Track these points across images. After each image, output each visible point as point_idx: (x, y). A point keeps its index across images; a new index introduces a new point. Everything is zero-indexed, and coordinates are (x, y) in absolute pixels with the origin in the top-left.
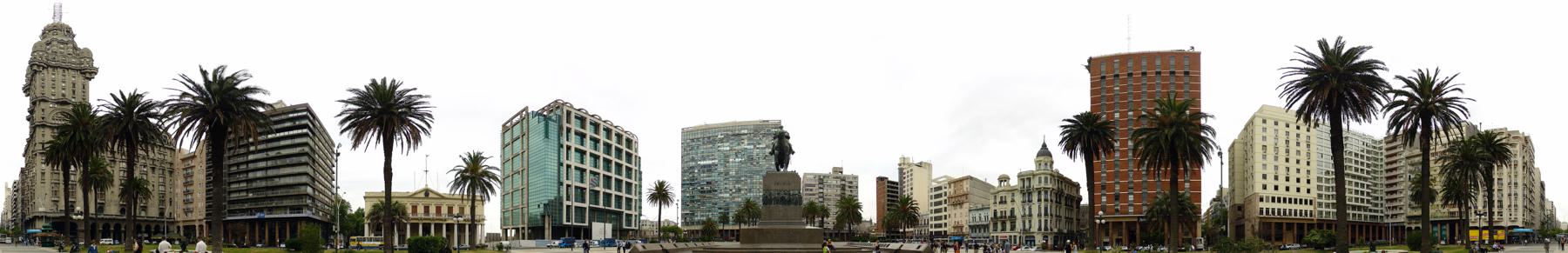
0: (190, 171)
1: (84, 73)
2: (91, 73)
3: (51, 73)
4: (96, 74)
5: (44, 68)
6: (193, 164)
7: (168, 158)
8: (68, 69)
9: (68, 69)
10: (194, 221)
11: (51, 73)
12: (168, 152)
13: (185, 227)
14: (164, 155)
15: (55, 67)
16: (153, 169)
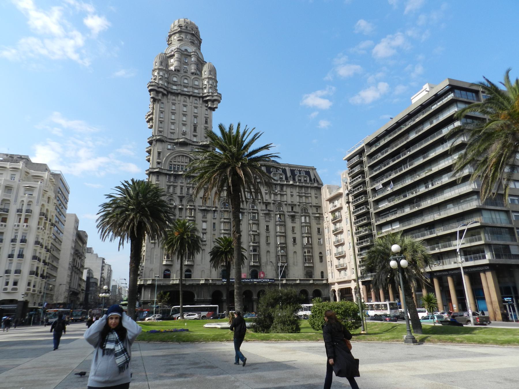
0: (337, 214)
1: (206, 102)
2: (213, 101)
3: (171, 101)
4: (219, 102)
5: (164, 95)
6: (338, 206)
7: (314, 202)
8: (189, 96)
9: (189, 96)
10: (349, 282)
11: (171, 101)
12: (313, 192)
13: (341, 290)
15: (177, 94)
16: (293, 217)
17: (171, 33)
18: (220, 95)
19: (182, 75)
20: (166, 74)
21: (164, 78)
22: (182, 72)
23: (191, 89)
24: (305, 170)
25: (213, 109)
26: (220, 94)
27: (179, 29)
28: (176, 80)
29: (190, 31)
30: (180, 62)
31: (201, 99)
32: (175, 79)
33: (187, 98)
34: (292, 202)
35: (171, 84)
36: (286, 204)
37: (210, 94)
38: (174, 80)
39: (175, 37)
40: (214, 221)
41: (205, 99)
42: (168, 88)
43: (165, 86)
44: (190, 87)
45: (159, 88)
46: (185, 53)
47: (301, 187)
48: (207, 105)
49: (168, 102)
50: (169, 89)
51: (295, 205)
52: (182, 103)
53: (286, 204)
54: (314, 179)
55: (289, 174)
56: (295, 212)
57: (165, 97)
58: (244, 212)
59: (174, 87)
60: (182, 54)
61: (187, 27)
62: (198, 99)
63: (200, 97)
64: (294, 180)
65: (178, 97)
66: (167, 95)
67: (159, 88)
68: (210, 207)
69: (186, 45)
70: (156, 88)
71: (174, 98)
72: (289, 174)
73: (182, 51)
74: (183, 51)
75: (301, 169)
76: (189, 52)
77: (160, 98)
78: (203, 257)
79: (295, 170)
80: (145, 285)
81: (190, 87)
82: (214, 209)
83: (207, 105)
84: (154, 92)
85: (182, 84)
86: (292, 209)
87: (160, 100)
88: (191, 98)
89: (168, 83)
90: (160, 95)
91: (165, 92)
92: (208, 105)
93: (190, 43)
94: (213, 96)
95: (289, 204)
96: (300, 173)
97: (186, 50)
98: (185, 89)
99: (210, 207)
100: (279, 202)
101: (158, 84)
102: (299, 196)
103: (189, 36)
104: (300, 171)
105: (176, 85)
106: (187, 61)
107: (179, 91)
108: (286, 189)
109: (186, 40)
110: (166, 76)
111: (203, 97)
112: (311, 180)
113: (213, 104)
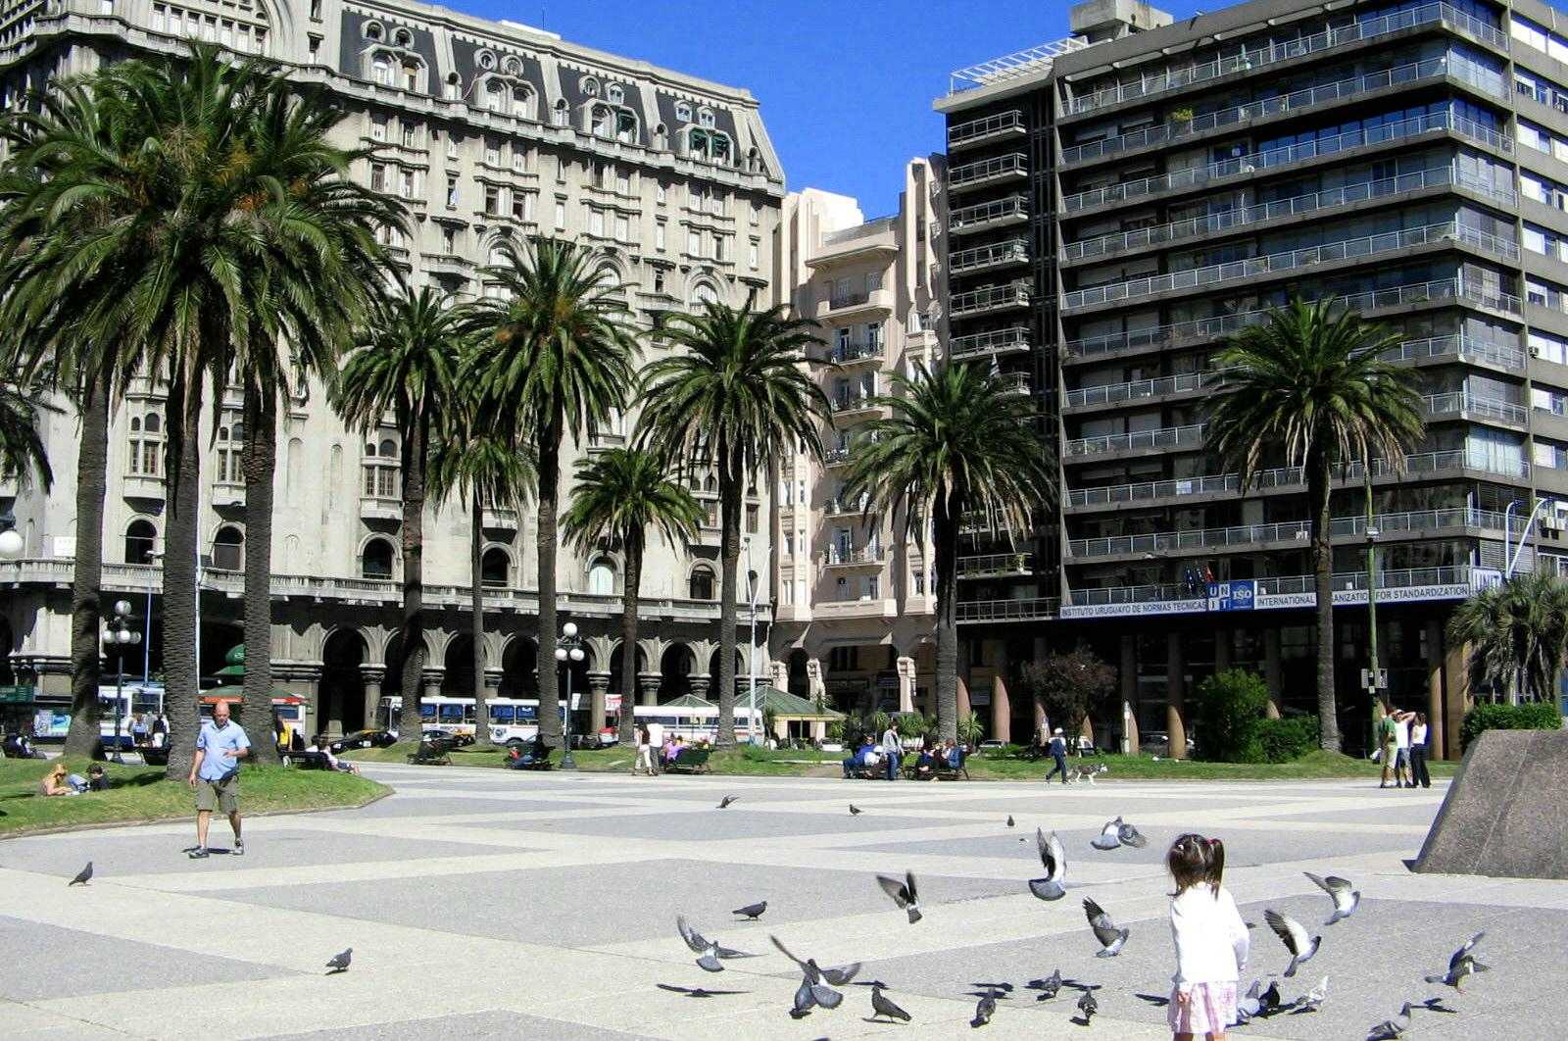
14: (719, 236)
24: (714, 103)
34: (660, 251)
36: (636, 260)
47: (700, 186)
51: (670, 267)
53: (636, 260)
54: (753, 153)
55: (653, 118)
56: (669, 299)
58: (468, 280)
64: (674, 146)
72: (653, 118)
75: (697, 99)
78: (293, 476)
79: (675, 98)
80: (58, 586)
86: (659, 284)
95: (648, 261)
96: (695, 120)
100: (611, 244)
102: (690, 225)
104: (695, 105)
108: (641, 187)
112: (737, 162)
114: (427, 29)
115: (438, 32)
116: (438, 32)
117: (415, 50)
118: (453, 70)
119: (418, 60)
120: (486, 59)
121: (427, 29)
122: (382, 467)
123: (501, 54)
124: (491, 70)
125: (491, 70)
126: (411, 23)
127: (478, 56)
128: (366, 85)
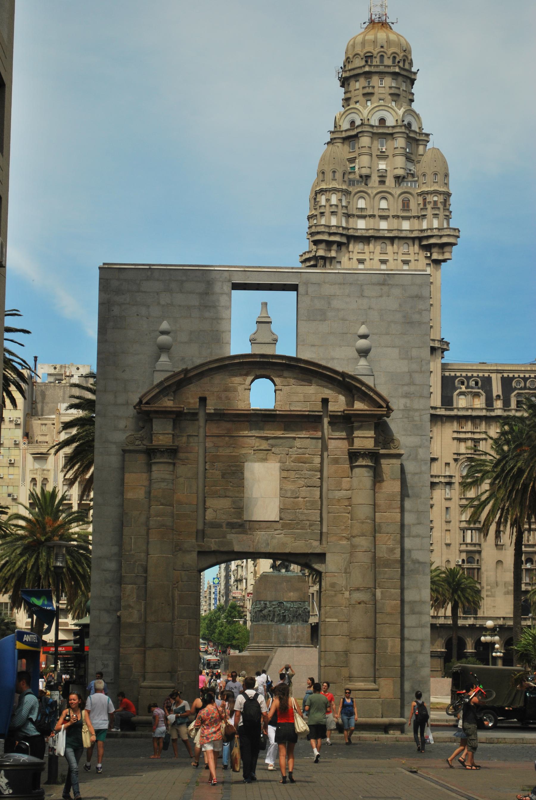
8: (392, 239)
9: (392, 239)
15: (366, 239)
17: (347, 74)
18: (456, 233)
19: (375, 192)
20: (344, 198)
21: (340, 207)
22: (375, 179)
23: (394, 224)
25: (445, 261)
26: (455, 229)
27: (367, 69)
28: (364, 206)
29: (389, 66)
30: (371, 155)
31: (417, 242)
32: (361, 204)
33: (388, 242)
35: (353, 215)
37: (436, 232)
38: (359, 206)
39: (357, 84)
40: (448, 504)
41: (425, 243)
42: (348, 229)
43: (344, 228)
44: (394, 217)
45: (330, 234)
46: (381, 131)
48: (429, 255)
49: (350, 259)
50: (351, 232)
52: (378, 257)
57: (344, 249)
59: (361, 224)
60: (373, 133)
61: (382, 56)
62: (410, 243)
63: (413, 239)
65: (369, 245)
66: (347, 245)
67: (330, 234)
68: (439, 476)
69: (381, 108)
70: (326, 237)
71: (359, 247)
73: (372, 126)
74: (377, 127)
76: (388, 127)
77: (333, 254)
81: (394, 217)
82: (447, 480)
83: (429, 255)
84: (323, 246)
85: (376, 213)
87: (334, 258)
88: (396, 241)
89: (348, 216)
90: (335, 247)
91: (344, 240)
92: (431, 254)
93: (389, 97)
94: (441, 237)
97: (382, 121)
98: (384, 225)
99: (439, 476)
101: (329, 227)
103: (388, 81)
105: (364, 217)
106: (384, 150)
107: (371, 233)
109: (382, 91)
110: (344, 204)
111: (420, 239)
113: (441, 251)
114: (489, 375)
115: (493, 376)
116: (493, 376)
117: (482, 388)
118: (500, 393)
119: (479, 392)
120: (518, 382)
121: (489, 375)
122: (467, 568)
123: (525, 379)
124: (521, 389)
125: (521, 389)
126: (481, 374)
127: (514, 384)
128: (452, 410)
